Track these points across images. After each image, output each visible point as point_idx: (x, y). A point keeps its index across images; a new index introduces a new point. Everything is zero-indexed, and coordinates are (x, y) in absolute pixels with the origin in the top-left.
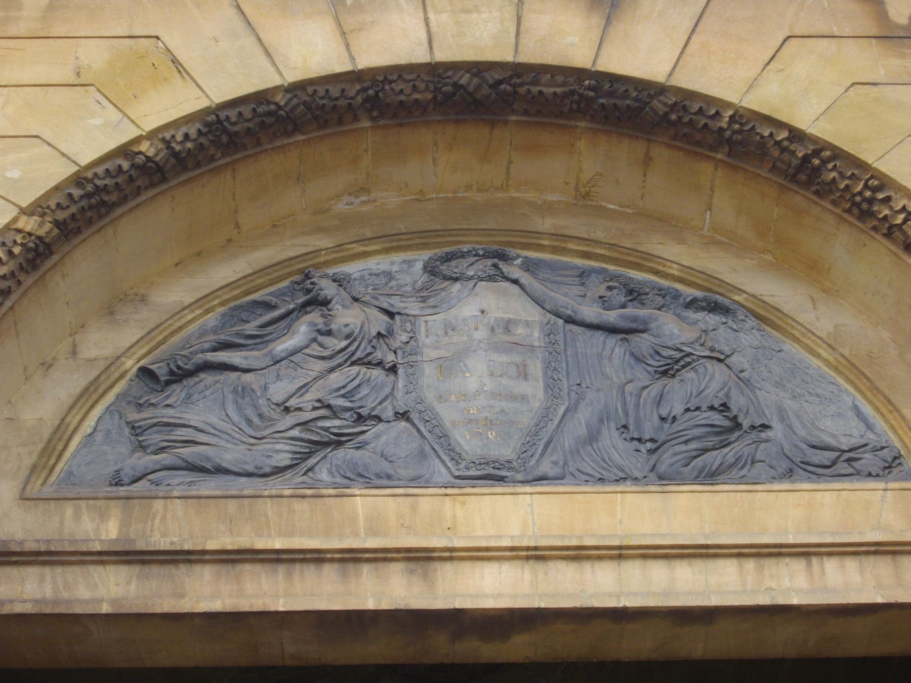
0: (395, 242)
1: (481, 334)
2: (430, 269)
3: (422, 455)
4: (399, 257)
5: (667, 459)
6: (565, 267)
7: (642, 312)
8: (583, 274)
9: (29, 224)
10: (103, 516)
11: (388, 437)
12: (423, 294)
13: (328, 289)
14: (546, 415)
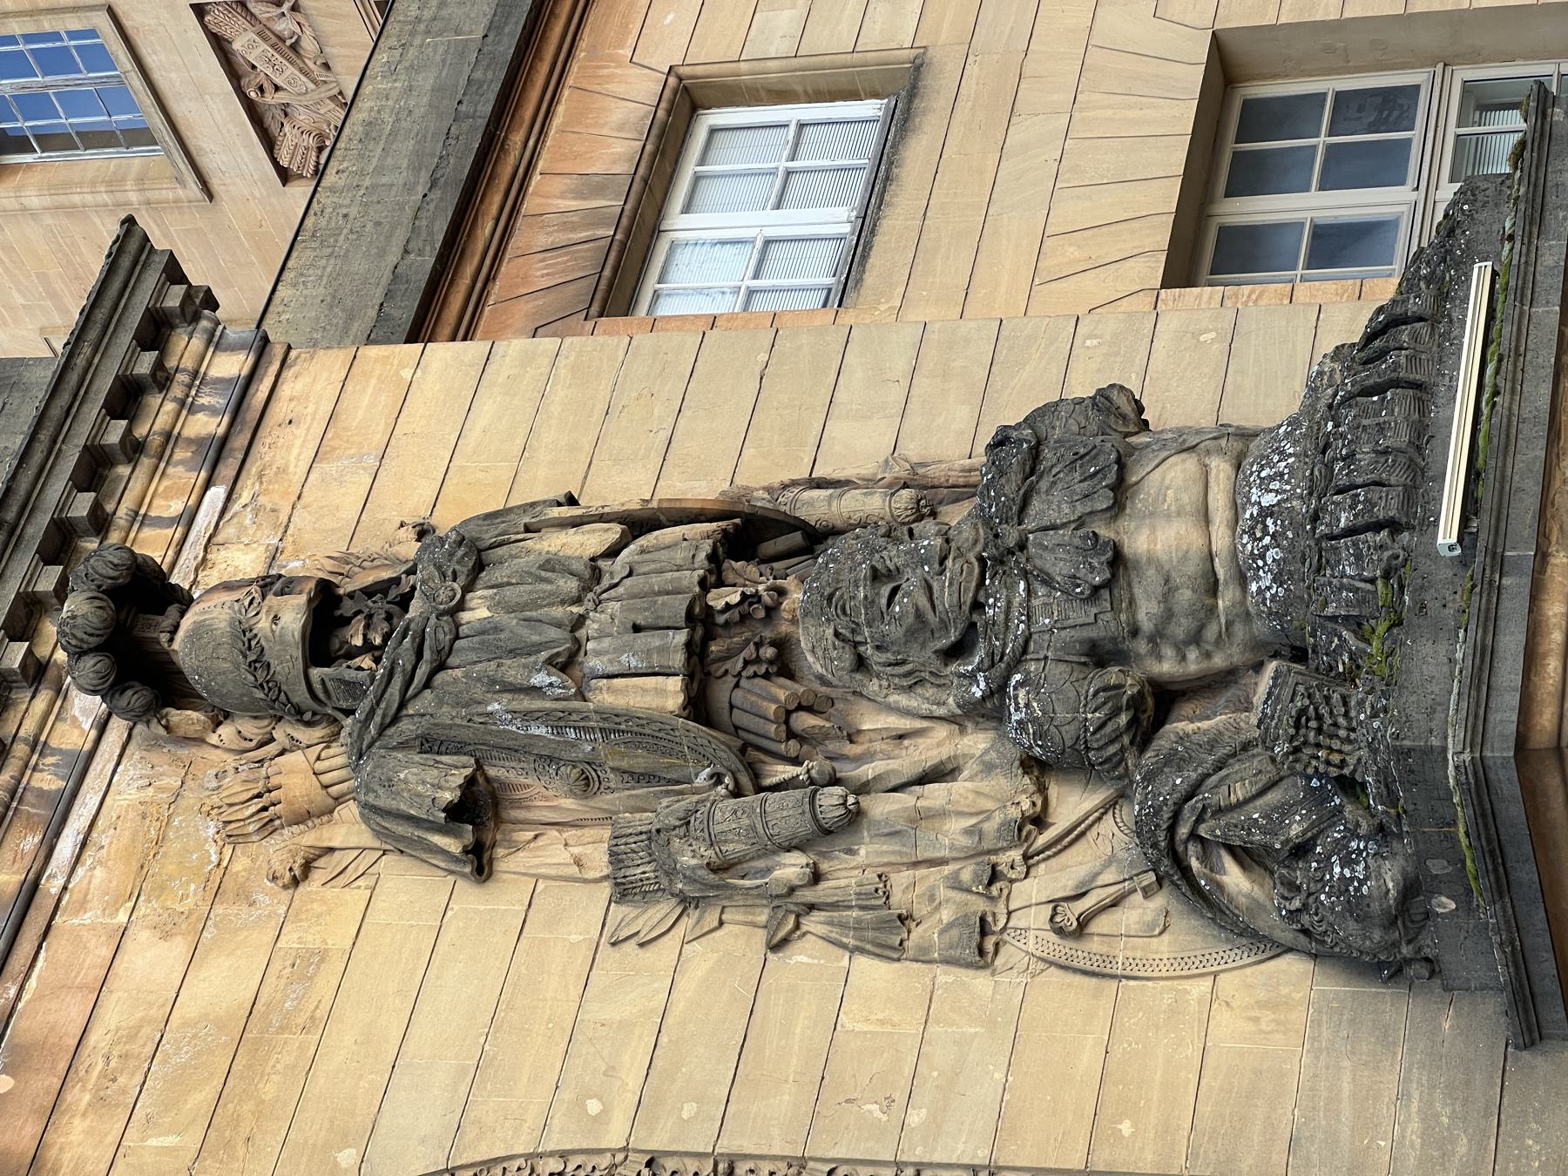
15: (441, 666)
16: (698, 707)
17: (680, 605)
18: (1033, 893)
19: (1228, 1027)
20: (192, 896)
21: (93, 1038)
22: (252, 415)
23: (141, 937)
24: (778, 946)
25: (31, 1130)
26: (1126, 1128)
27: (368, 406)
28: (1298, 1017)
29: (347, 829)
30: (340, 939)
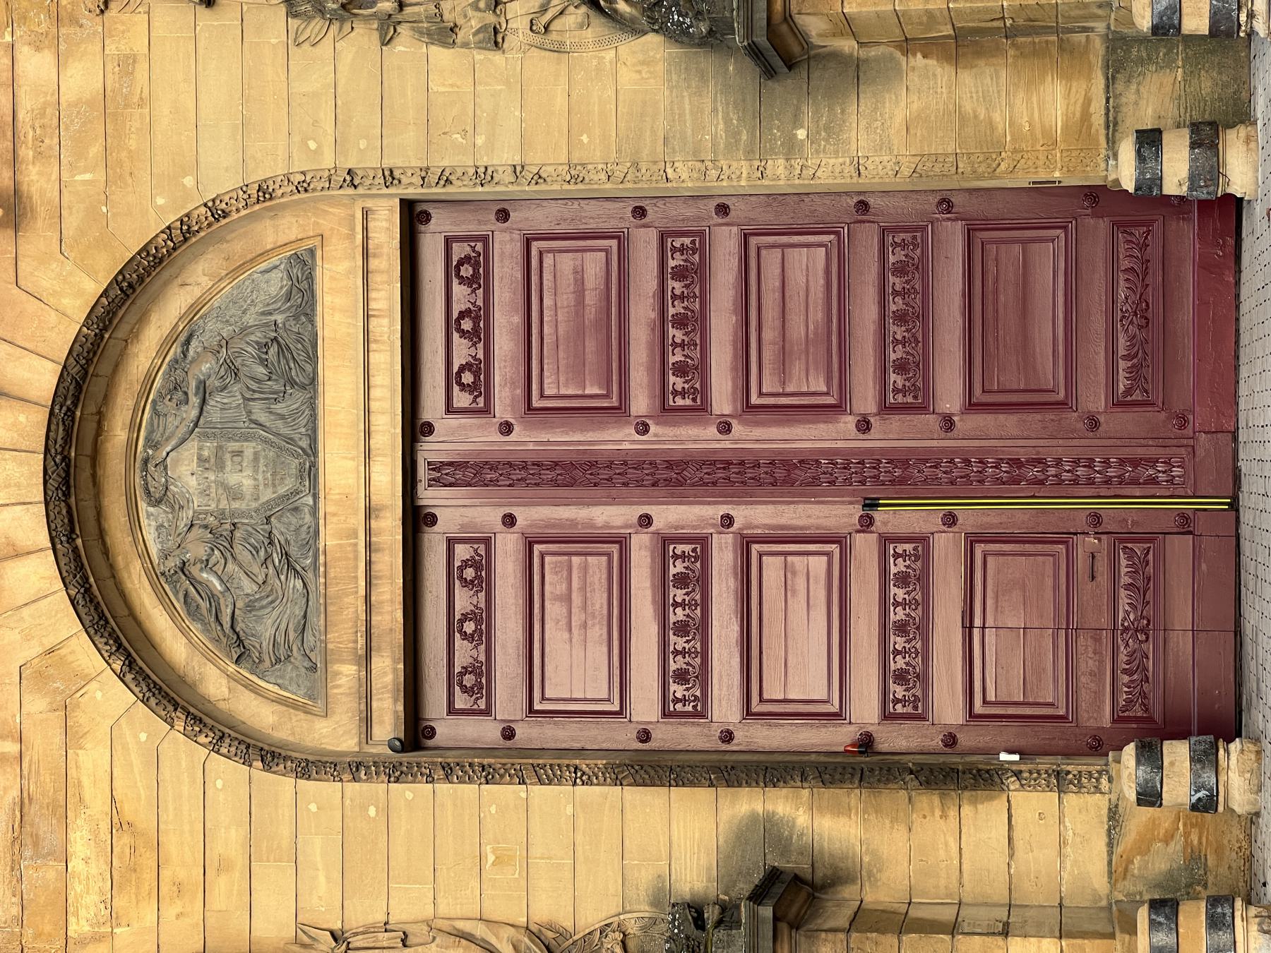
2: (157, 503)
3: (296, 509)
4: (144, 521)
7: (193, 384)
8: (155, 412)
9: (179, 725)
10: (337, 674)
12: (177, 508)
13: (172, 563)
14: (265, 441)
19: (627, 76)
20: (43, 23)
21: (21, 115)
23: (24, 52)
24: (386, 42)
26: (585, 138)
28: (660, 68)
30: (140, 46)
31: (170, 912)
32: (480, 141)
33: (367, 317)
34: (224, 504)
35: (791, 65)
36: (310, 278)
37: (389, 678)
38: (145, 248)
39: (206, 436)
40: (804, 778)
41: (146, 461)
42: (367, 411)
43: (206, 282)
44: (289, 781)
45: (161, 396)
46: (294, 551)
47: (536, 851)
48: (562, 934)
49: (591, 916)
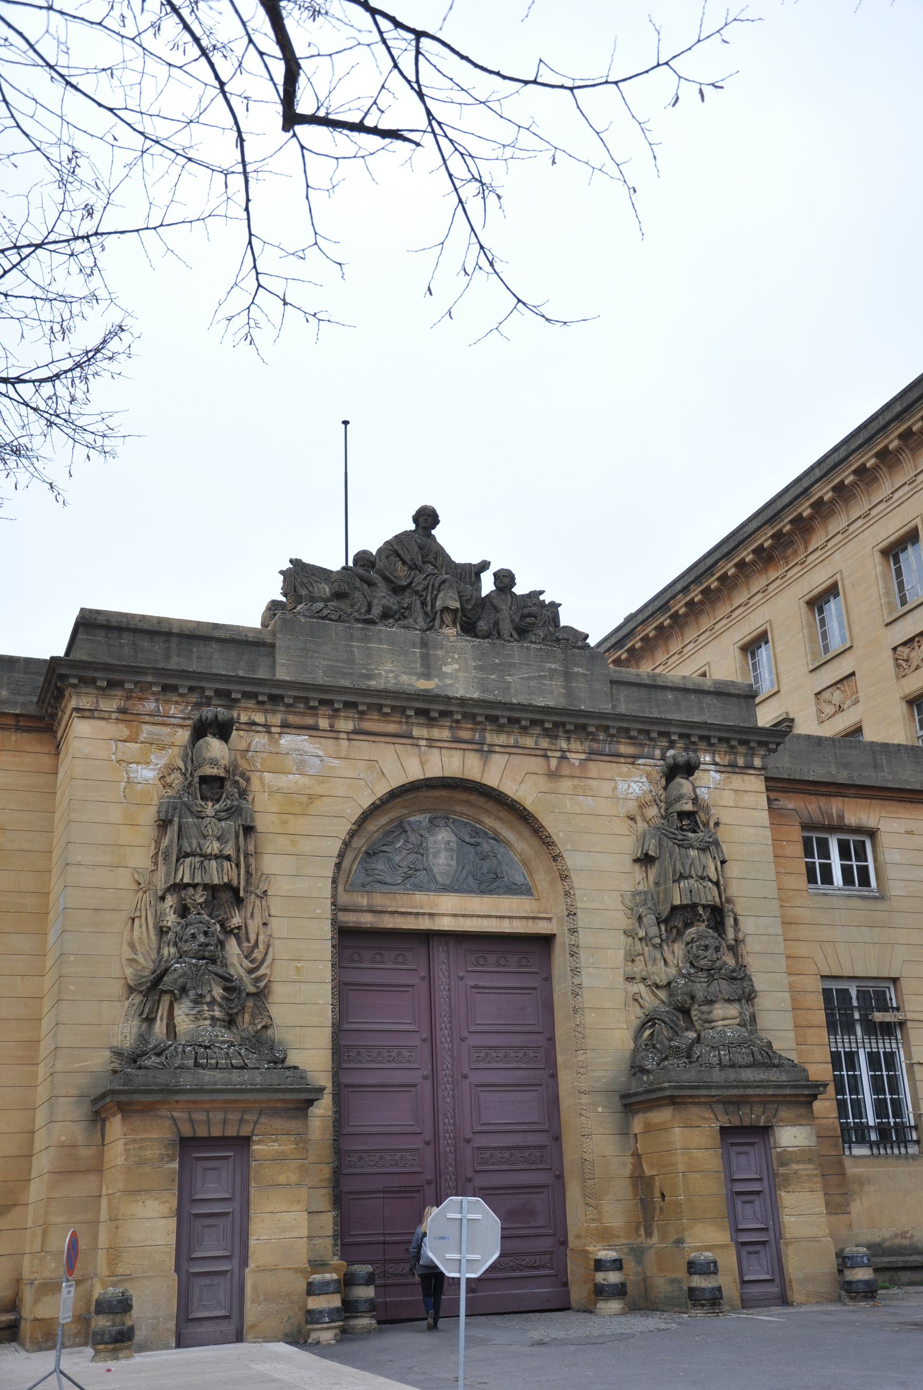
0: (422, 811)
1: (443, 846)
2: (431, 821)
4: (422, 816)
5: (482, 887)
6: (462, 821)
7: (479, 840)
8: (466, 824)
10: (363, 897)
11: (422, 875)
12: (429, 830)
13: (408, 828)
14: (457, 870)
15: (679, 846)
16: (674, 909)
17: (697, 901)
18: (642, 988)
19: (618, 1033)
22: (744, 771)
25: (567, 773)
27: (749, 800)
29: (641, 826)
31: (274, 818)
32: (590, 970)
33: (510, 918)
34: (431, 850)
35: (625, 1105)
36: (522, 893)
37: (362, 920)
38: (542, 827)
39: (458, 845)
40: (335, 1112)
41: (448, 818)
42: (472, 916)
43: (519, 849)
44: (331, 875)
45: (473, 826)
46: (412, 880)
47: (303, 986)
48: (266, 997)
49: (274, 1010)
